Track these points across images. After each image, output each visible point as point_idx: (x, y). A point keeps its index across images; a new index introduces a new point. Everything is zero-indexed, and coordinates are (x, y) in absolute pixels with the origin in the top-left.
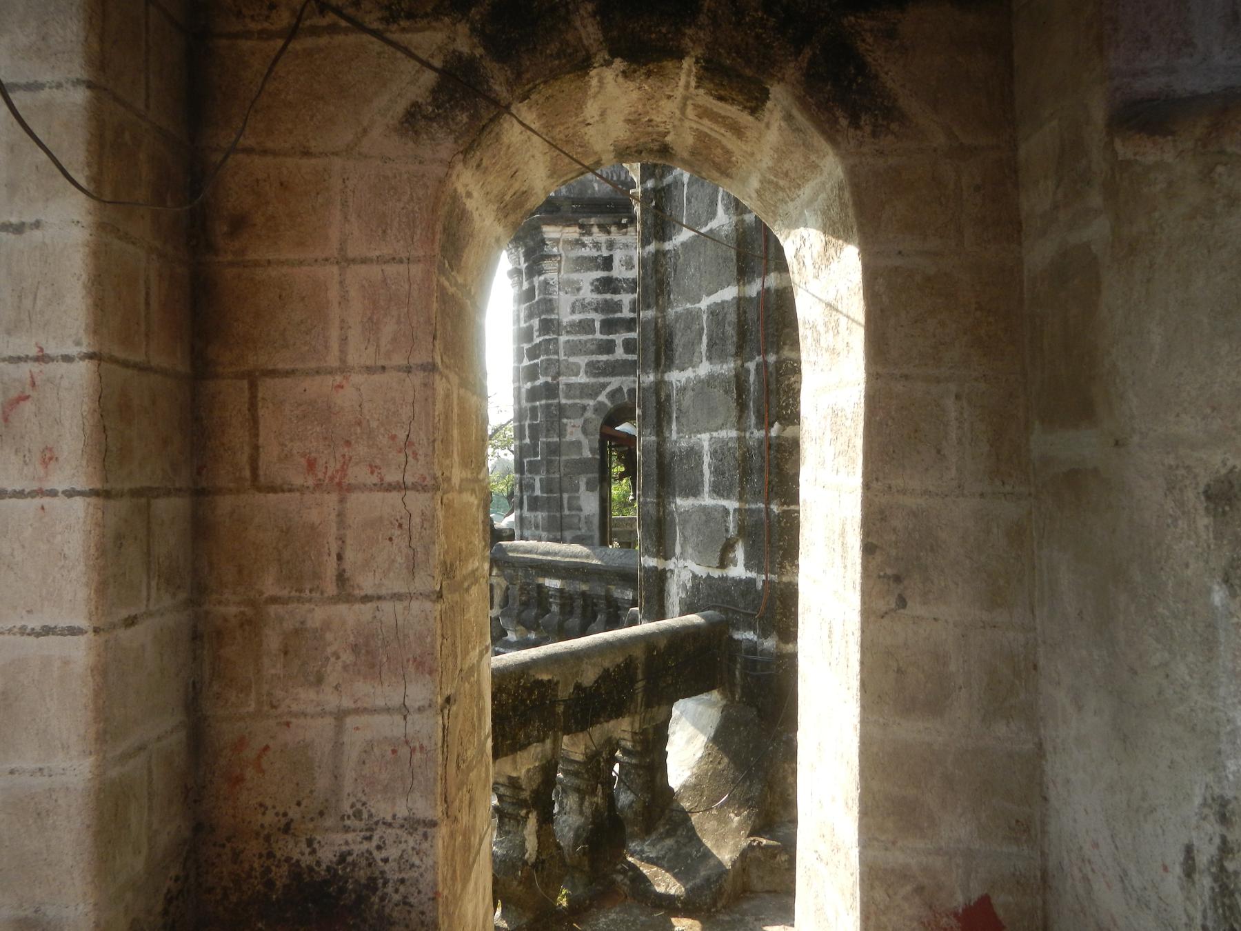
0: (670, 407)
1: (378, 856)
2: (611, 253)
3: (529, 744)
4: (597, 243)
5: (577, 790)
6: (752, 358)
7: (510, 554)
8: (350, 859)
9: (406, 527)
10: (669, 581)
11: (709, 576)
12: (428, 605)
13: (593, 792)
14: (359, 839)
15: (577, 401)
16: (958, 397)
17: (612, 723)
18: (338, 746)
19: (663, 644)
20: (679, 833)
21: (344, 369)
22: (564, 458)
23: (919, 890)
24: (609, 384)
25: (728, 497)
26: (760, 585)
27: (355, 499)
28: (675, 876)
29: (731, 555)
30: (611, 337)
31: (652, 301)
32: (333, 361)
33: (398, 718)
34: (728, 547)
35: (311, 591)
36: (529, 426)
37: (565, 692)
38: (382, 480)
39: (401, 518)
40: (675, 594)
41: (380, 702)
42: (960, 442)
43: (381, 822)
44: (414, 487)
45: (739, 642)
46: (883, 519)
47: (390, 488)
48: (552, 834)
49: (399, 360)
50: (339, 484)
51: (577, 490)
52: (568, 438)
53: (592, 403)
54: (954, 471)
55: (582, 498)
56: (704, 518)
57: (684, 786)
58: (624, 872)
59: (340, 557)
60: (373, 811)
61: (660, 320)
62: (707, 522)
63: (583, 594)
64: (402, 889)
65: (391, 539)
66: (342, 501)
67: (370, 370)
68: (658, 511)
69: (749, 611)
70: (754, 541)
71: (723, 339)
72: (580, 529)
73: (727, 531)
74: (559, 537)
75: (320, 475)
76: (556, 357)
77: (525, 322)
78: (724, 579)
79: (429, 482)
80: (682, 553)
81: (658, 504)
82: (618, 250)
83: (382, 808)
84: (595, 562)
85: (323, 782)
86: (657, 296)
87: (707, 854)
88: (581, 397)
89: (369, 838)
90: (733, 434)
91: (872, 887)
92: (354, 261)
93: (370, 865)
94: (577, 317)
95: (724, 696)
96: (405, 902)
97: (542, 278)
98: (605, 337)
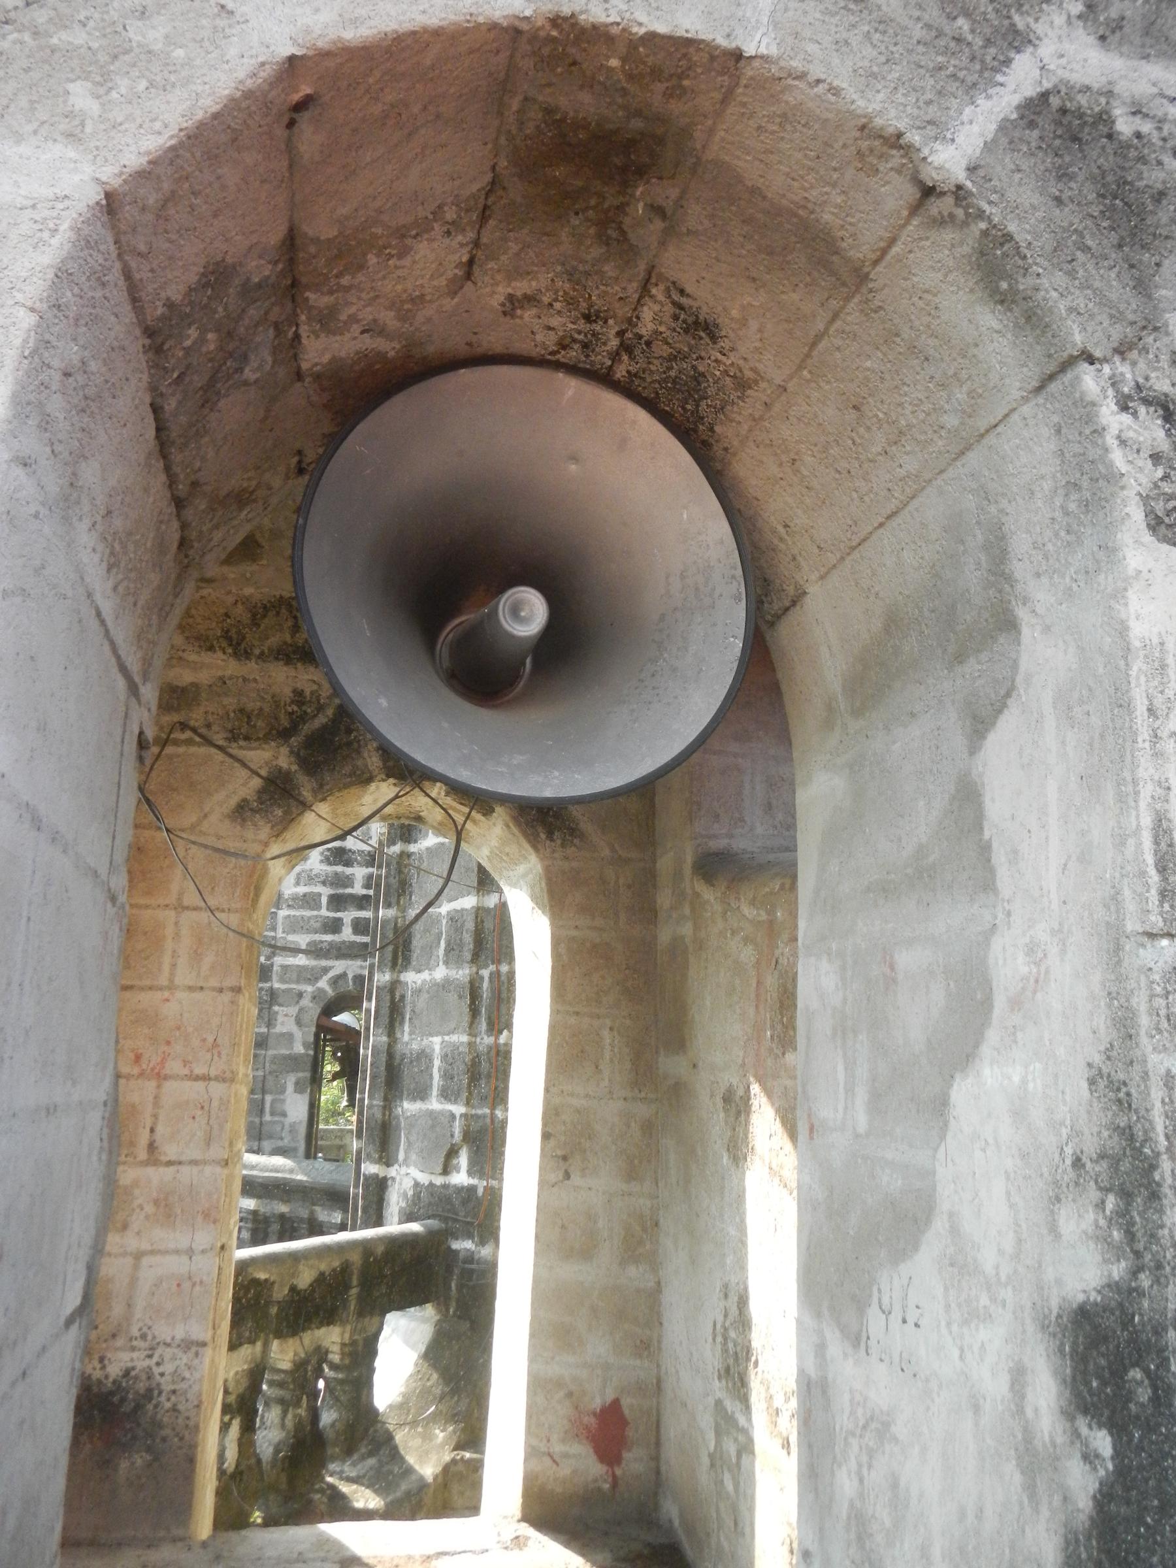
0: (404, 1007)
3: (241, 1345)
5: (281, 1401)
6: (486, 966)
8: (133, 1373)
9: (206, 1108)
10: (390, 1189)
11: (431, 1184)
12: (218, 1170)
13: (298, 1404)
14: (142, 1356)
16: (611, 1029)
17: (323, 1330)
18: (133, 1281)
19: (380, 1250)
20: (381, 1452)
21: (171, 987)
22: (271, 1052)
23: (570, 1395)
24: (331, 968)
25: (455, 1102)
26: (480, 1191)
27: (169, 1086)
28: (376, 1492)
29: (455, 1162)
30: (339, 915)
31: (394, 900)
32: (163, 980)
33: (185, 1258)
34: (452, 1153)
35: (126, 1156)
37: (280, 1293)
40: (395, 1202)
41: (172, 1246)
42: (611, 1061)
44: (217, 1079)
45: (456, 1252)
46: (557, 1114)
47: (197, 1078)
48: (252, 1443)
49: (214, 982)
50: (158, 1074)
51: (283, 1091)
52: (279, 1029)
53: (309, 989)
54: (607, 1080)
55: (288, 1101)
56: (430, 1122)
57: (390, 1406)
58: (322, 1491)
59: (152, 1130)
60: (156, 1333)
62: (433, 1127)
63: (282, 1217)
64: (173, 1398)
66: (159, 1087)
67: (191, 989)
68: (384, 1115)
69: (469, 1219)
70: (478, 1147)
71: (461, 945)
72: (282, 1139)
73: (452, 1136)
74: (255, 1148)
75: (144, 1066)
76: (272, 934)
78: (445, 1186)
79: (228, 1075)
80: (405, 1160)
81: (384, 1107)
83: (163, 1331)
84: (300, 1177)
85: (118, 1310)
86: (399, 896)
87: (409, 1471)
88: (298, 982)
89: (150, 1356)
90: (465, 1038)
91: (535, 1394)
92: (187, 908)
93: (149, 1378)
94: (302, 890)
95: (439, 1311)
96: (174, 1409)
98: (332, 915)
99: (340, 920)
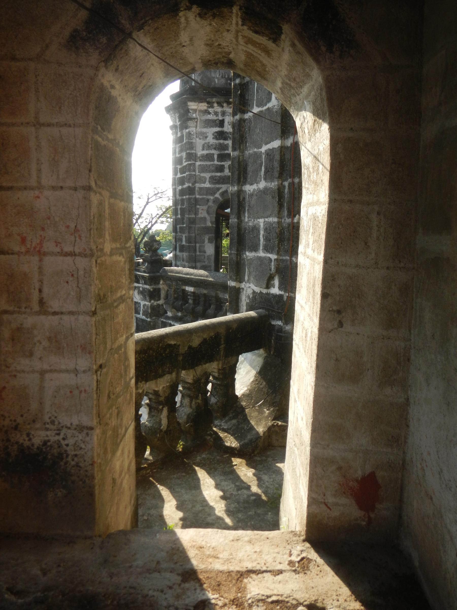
0: (245, 204)
1: (63, 443)
2: (224, 118)
3: (164, 375)
4: (216, 112)
5: (189, 396)
6: (286, 180)
7: (169, 274)
8: (49, 444)
9: (75, 276)
10: (242, 293)
11: (261, 292)
12: (88, 318)
13: (197, 398)
14: (53, 434)
15: (205, 197)
16: (379, 213)
17: (207, 365)
18: (42, 388)
19: (235, 326)
20: (239, 417)
21: (40, 187)
22: (197, 226)
23: (340, 468)
24: (221, 188)
25: (272, 253)
26: (285, 298)
27: (48, 260)
28: (235, 438)
29: (272, 282)
30: (223, 163)
31: (237, 147)
32: (33, 182)
33: (73, 375)
34: (271, 278)
35: (25, 308)
36: (180, 208)
37: (183, 350)
38: (62, 250)
39: (73, 271)
40: (244, 300)
41: (63, 367)
42: (378, 238)
43: (64, 427)
44: (80, 255)
45: (274, 326)
46: (334, 280)
47: (67, 254)
48: (175, 417)
49: (69, 183)
50: (39, 251)
51: (204, 242)
52: (200, 216)
54: (373, 255)
55: (206, 246)
56: (259, 263)
57: (243, 395)
58: (210, 435)
59: (40, 291)
60: (60, 421)
61: (241, 157)
62: (261, 265)
63: (205, 295)
64: (76, 459)
65: (67, 282)
66: (41, 260)
67: (54, 188)
68: (237, 258)
69: (280, 311)
70: (283, 276)
71: (273, 169)
72: (204, 262)
73: (270, 270)
74: (194, 266)
75: (29, 246)
76: (194, 173)
77: (179, 154)
78: (268, 294)
79: (88, 252)
80: (248, 280)
81: (237, 254)
82: (227, 117)
83: (65, 420)
84: (210, 279)
85: (34, 406)
86: (240, 144)
87: (252, 428)
88: (207, 195)
89: (58, 434)
90: (276, 220)
91: (316, 467)
92: (43, 125)
93: (59, 447)
94: (205, 152)
95: (266, 352)
96: (77, 465)
97: (187, 130)
98: (219, 163)
99: (223, 166)
